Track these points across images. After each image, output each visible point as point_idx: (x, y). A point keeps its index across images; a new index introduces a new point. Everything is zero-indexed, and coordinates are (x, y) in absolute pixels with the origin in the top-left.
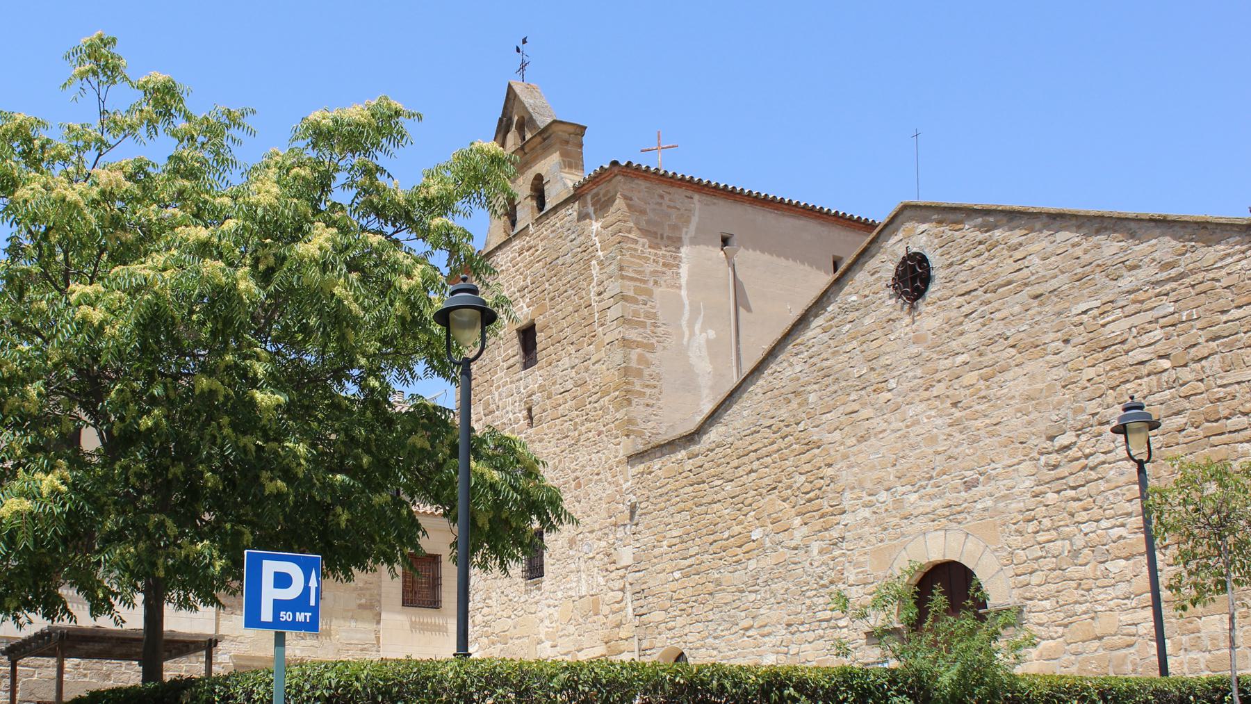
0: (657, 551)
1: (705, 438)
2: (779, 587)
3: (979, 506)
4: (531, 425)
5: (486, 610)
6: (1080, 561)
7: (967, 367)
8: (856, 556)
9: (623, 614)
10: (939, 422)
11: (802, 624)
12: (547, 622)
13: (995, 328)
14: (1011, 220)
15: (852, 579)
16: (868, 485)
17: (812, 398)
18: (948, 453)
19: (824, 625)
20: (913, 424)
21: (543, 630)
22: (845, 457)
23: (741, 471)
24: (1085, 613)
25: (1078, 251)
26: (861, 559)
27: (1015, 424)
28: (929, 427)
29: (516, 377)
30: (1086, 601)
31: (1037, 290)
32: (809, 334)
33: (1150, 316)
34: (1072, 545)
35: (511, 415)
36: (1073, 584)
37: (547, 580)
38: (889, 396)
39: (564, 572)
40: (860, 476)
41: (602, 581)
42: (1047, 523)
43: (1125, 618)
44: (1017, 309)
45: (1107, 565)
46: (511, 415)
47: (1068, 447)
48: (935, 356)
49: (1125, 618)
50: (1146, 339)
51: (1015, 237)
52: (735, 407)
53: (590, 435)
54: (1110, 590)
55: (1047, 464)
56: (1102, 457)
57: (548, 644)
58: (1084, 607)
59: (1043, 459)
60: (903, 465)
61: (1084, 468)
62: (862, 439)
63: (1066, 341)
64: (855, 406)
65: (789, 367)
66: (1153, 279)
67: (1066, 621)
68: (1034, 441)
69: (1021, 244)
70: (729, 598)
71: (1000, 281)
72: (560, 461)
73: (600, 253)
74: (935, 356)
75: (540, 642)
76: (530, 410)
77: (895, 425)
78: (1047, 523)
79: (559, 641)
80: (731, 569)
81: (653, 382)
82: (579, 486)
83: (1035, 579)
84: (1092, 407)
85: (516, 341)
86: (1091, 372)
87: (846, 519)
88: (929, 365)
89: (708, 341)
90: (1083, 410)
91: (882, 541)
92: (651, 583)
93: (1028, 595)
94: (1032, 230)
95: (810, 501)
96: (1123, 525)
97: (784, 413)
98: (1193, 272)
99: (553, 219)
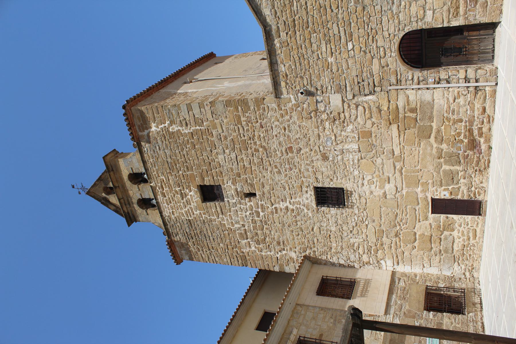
1: (268, 20)
4: (254, 195)
5: (361, 251)
9: (372, 105)
12: (373, 187)
29: (227, 205)
35: (248, 213)
37: (348, 186)
46: (248, 213)
53: (262, 135)
57: (387, 187)
72: (276, 167)
73: (166, 125)
79: (386, 174)
85: (208, 203)
92: (354, 73)
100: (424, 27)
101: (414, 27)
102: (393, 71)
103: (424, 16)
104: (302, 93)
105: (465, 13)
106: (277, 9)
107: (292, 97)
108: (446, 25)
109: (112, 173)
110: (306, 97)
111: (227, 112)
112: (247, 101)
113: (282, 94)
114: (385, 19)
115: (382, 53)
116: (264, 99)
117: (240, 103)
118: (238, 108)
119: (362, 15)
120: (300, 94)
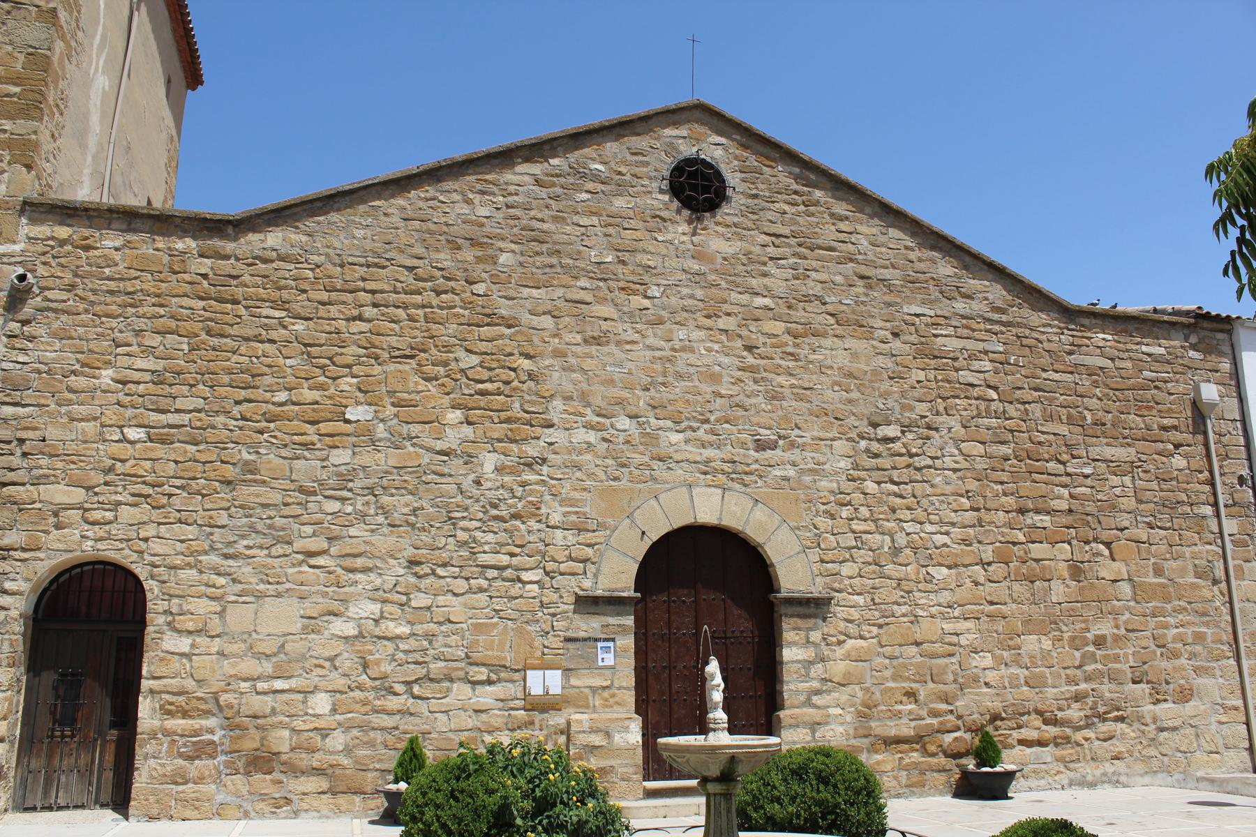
1: (253, 237)
2: (400, 504)
3: (777, 472)
6: (900, 560)
7: (770, 314)
8: (566, 489)
10: (726, 360)
11: (444, 565)
14: (837, 189)
16: (597, 401)
17: (503, 258)
18: (736, 399)
19: (492, 573)
20: (683, 349)
24: (904, 615)
25: (913, 255)
26: (577, 495)
27: (833, 398)
28: (706, 361)
30: (905, 604)
31: (863, 270)
32: (508, 176)
33: (981, 346)
34: (893, 541)
38: (647, 303)
40: (585, 386)
42: (864, 511)
43: (948, 627)
45: (930, 569)
48: (723, 284)
49: (948, 627)
50: (976, 365)
51: (841, 208)
52: (334, 217)
54: (932, 596)
55: (867, 451)
56: (929, 462)
58: (904, 609)
60: (662, 395)
61: (908, 466)
62: (596, 341)
63: (896, 335)
64: (588, 297)
65: (459, 204)
66: (986, 315)
67: (881, 621)
68: (852, 421)
69: (847, 218)
70: (276, 498)
71: (820, 242)
74: (723, 284)
77: (651, 341)
80: (284, 453)
83: (847, 569)
84: (922, 408)
86: (921, 375)
88: (713, 290)
90: (912, 409)
91: (616, 479)
92: (52, 433)
93: (836, 585)
94: (861, 211)
95: (483, 393)
96: (947, 533)
98: (1019, 325)
100: (150, 629)
101: (156, 605)
102: (38, 538)
103: (179, 632)
104: (22, 278)
105: (167, 733)
106: (274, 265)
107: (17, 248)
108: (145, 684)
110: (7, 286)
111: (10, 48)
112: (33, 119)
113: (33, 221)
114: (190, 532)
115: (97, 515)
116: (29, 167)
117: (31, 96)
118: (16, 85)
119: (212, 475)
120: (21, 271)
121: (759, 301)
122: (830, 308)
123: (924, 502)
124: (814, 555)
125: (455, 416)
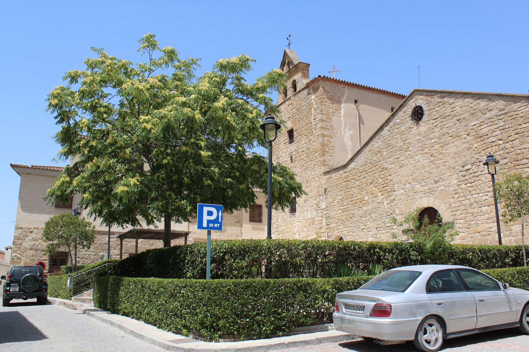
0: (333, 204)
2: (373, 215)
4: (292, 162)
5: (277, 223)
6: (473, 207)
8: (399, 206)
10: (426, 161)
12: (297, 227)
13: (445, 130)
14: (450, 95)
15: (397, 213)
16: (403, 182)
17: (384, 153)
19: (389, 228)
21: (296, 230)
22: (395, 173)
23: (361, 178)
25: (472, 105)
26: (401, 206)
27: (451, 162)
28: (423, 163)
29: (287, 146)
31: (458, 118)
32: (384, 132)
33: (496, 126)
36: (471, 215)
37: (297, 213)
38: (410, 153)
39: (303, 211)
41: (315, 213)
42: (462, 194)
43: (488, 226)
44: (452, 124)
47: (469, 170)
48: (425, 140)
49: (488, 226)
50: (494, 134)
51: (451, 100)
52: (359, 156)
54: (482, 217)
55: (462, 175)
56: (480, 173)
57: (297, 234)
58: (474, 222)
59: (461, 173)
60: (414, 175)
61: (474, 176)
62: (401, 167)
63: (468, 135)
64: (399, 156)
65: (377, 143)
66: (497, 114)
70: (357, 219)
71: (446, 115)
73: (315, 106)
74: (425, 140)
75: (295, 234)
76: (291, 157)
77: (412, 162)
78: (462, 194)
79: (301, 233)
81: (332, 148)
82: (308, 182)
83: (458, 213)
84: (477, 156)
85: (287, 135)
86: (476, 145)
87: (395, 193)
89: (350, 135)
90: (474, 157)
92: (332, 214)
93: (455, 218)
94: (457, 98)
95: (384, 187)
96: (487, 195)
97: (375, 158)
98: (510, 112)
99: (299, 95)
109: (294, 68)
114: (348, 228)
121: (433, 141)
122: (450, 135)
123: (479, 187)
124: (450, 210)
125: (380, 194)
